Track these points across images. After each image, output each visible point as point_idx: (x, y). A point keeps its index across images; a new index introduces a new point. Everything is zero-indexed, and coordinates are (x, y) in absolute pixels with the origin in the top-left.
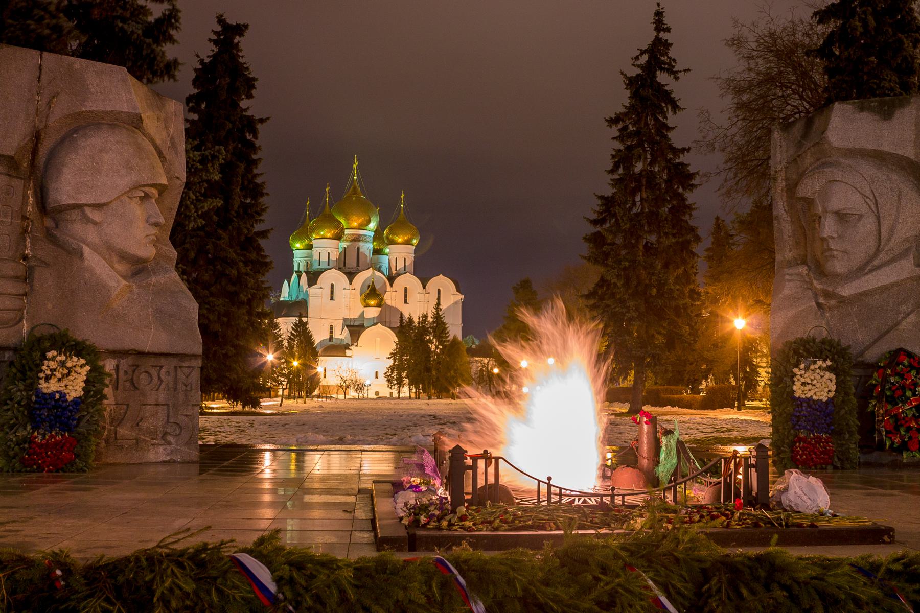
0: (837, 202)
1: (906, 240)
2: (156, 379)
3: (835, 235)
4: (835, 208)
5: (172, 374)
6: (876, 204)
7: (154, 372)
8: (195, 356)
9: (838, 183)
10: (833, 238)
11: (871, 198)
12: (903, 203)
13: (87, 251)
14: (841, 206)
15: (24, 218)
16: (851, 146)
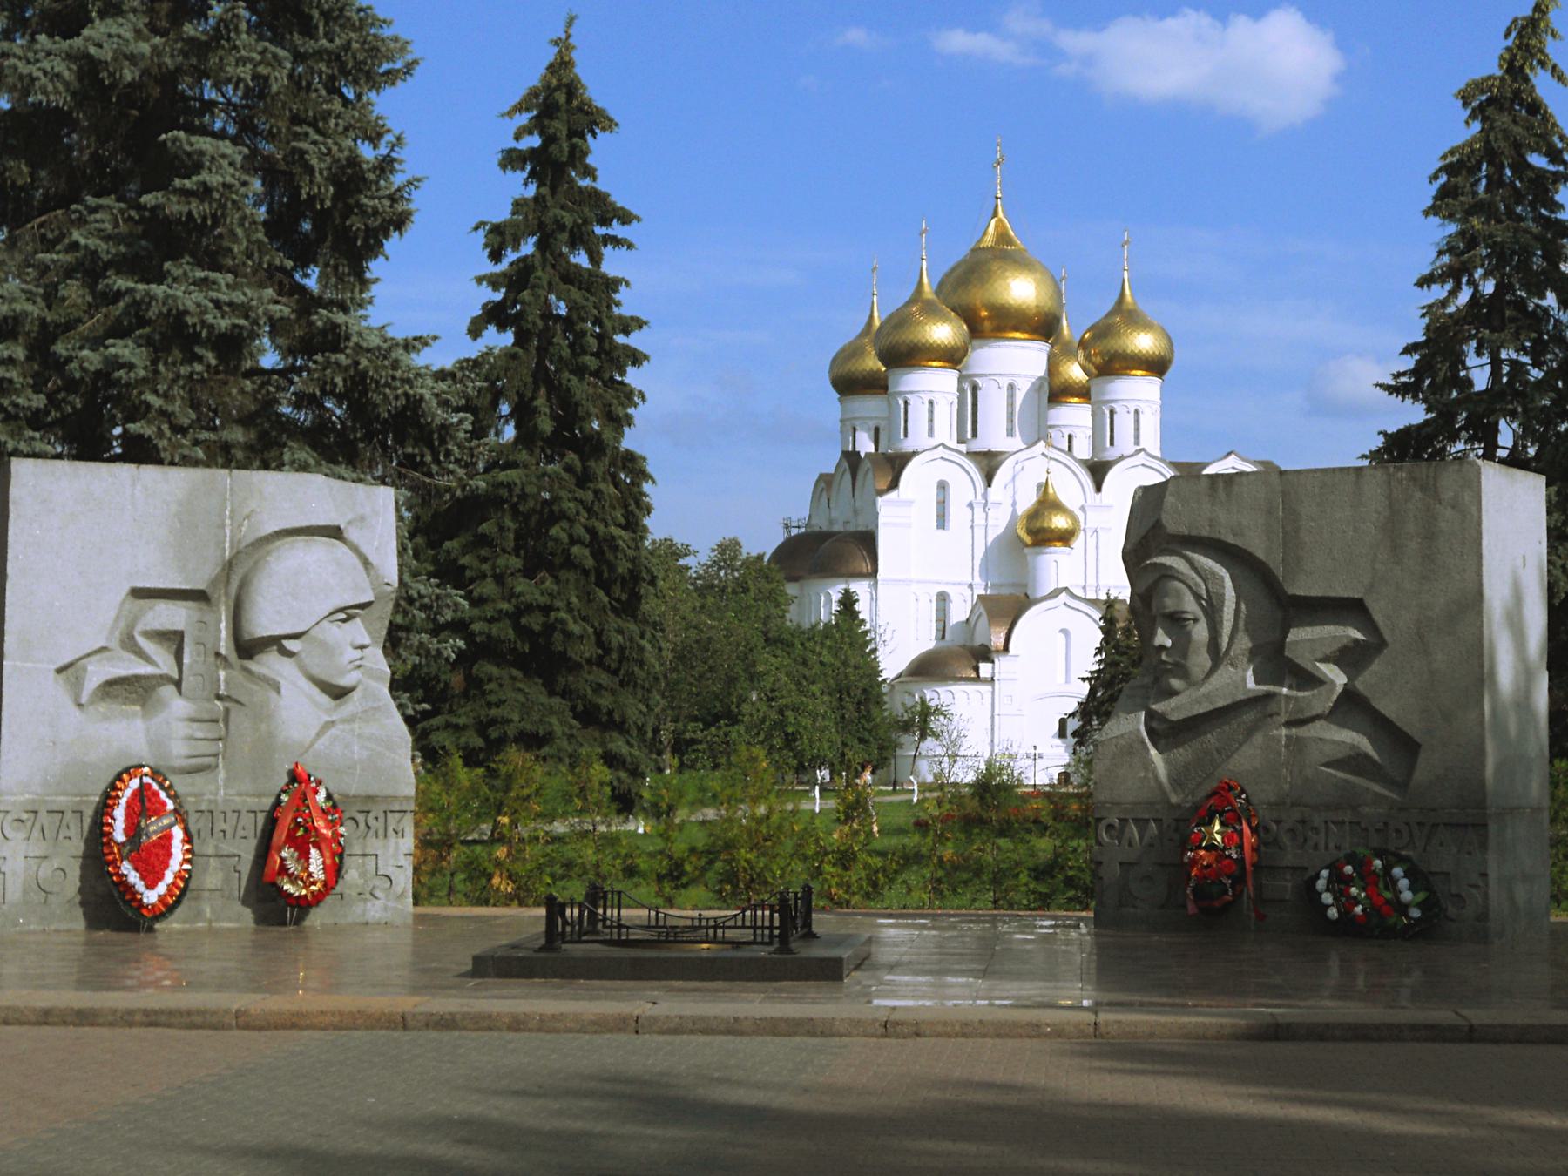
2: (362, 825)
5: (382, 819)
7: (361, 818)
8: (407, 798)
15: (218, 655)
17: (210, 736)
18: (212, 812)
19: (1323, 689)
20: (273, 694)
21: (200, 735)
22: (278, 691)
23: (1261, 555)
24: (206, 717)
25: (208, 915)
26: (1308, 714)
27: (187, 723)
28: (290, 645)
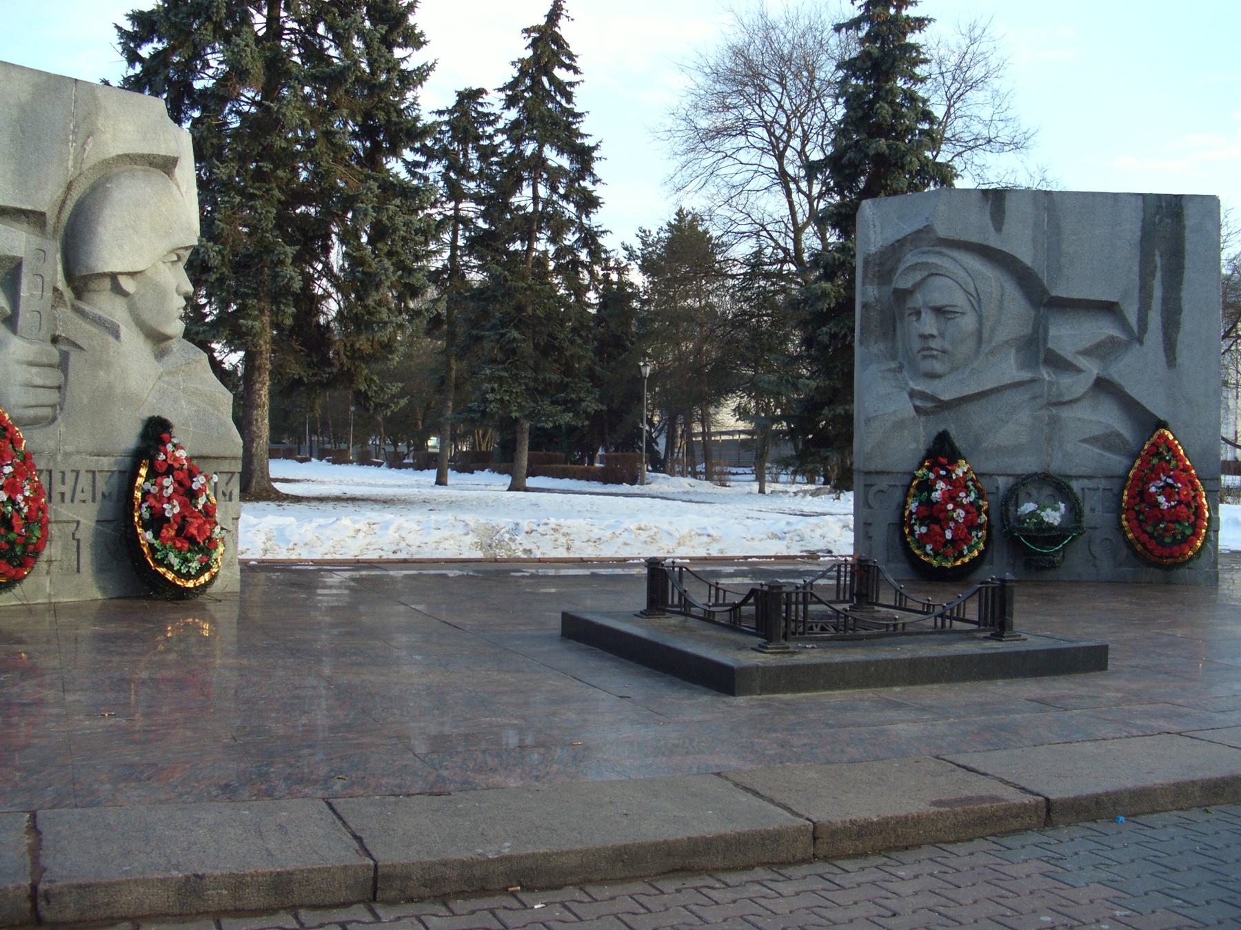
0: (939, 299)
1: (1007, 342)
3: (935, 332)
4: (938, 304)
6: (979, 301)
8: (234, 458)
9: (943, 278)
10: (932, 336)
11: (975, 295)
12: (1006, 304)
13: (124, 331)
14: (944, 302)
16: (957, 238)
17: (48, 383)
18: (50, 472)
19: (1081, 376)
20: (112, 339)
21: (39, 381)
22: (117, 337)
23: (1027, 259)
24: (45, 360)
25: (48, 590)
26: (1066, 398)
27: (25, 366)
28: (127, 284)
